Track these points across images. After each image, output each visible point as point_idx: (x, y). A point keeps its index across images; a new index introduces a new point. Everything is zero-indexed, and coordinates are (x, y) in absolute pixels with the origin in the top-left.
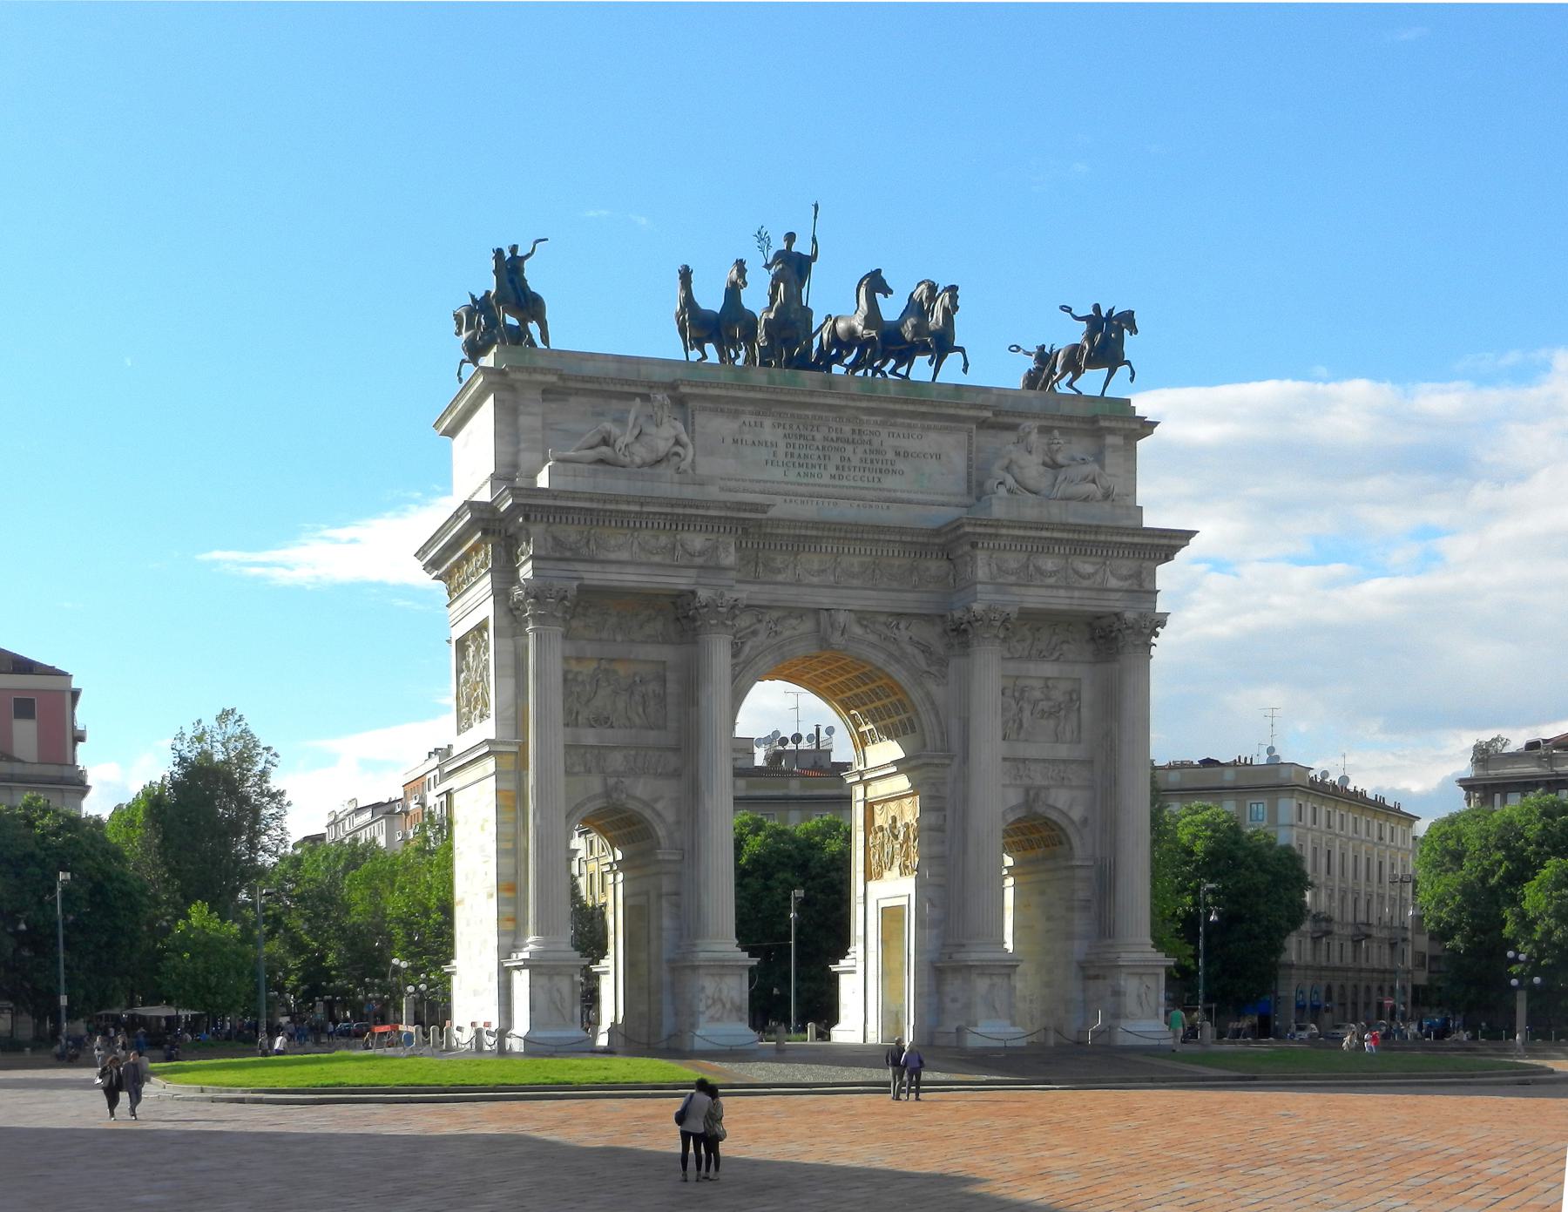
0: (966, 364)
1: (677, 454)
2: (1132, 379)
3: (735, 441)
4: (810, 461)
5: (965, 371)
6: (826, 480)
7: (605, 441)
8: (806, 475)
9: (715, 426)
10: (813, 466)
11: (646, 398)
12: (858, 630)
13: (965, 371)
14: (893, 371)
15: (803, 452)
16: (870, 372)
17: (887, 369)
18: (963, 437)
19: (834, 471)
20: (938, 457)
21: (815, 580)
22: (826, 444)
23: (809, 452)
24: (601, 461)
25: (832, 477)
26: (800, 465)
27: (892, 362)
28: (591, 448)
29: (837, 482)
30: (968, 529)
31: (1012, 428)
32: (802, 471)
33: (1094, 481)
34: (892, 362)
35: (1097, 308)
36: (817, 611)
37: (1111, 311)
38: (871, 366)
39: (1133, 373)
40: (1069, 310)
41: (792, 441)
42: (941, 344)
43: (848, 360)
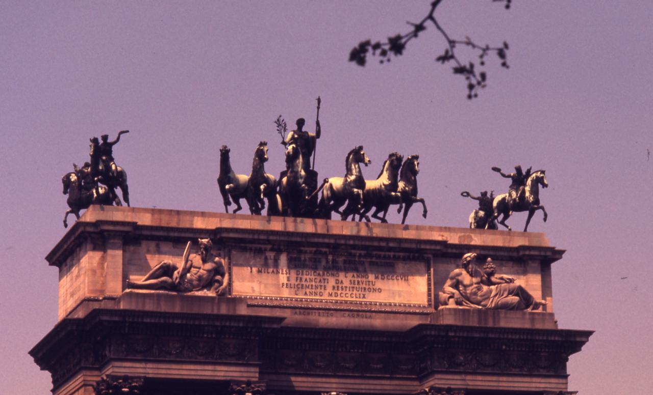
0: (425, 212)
2: (545, 220)
5: (425, 216)
6: (326, 297)
8: (311, 294)
10: (316, 287)
13: (425, 216)
14: (375, 216)
16: (357, 217)
17: (370, 214)
25: (331, 295)
26: (307, 287)
27: (374, 209)
32: (308, 291)
34: (374, 209)
35: (518, 170)
38: (359, 213)
39: (546, 215)
43: (342, 209)
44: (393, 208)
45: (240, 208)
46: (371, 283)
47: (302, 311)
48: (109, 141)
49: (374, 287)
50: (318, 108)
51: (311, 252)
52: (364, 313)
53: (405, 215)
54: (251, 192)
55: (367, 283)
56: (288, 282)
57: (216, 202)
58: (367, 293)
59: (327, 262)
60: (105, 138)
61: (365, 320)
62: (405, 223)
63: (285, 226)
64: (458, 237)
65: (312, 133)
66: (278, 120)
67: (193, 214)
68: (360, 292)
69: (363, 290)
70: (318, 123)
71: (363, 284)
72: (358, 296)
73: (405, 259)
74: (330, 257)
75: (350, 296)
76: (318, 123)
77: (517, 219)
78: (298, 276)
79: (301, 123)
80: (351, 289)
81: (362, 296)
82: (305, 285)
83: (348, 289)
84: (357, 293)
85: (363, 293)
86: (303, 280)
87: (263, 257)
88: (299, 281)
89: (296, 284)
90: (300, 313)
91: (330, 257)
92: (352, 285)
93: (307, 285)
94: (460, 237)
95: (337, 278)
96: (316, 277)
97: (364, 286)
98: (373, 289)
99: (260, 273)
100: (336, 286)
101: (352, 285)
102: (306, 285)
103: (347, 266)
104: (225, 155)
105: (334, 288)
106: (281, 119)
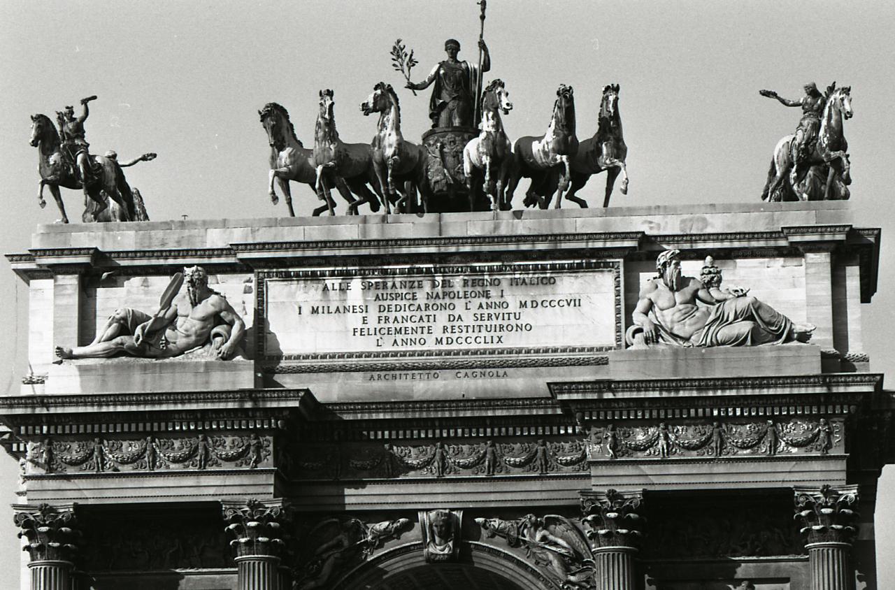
1: (218, 335)
3: (315, 311)
4: (409, 324)
6: (431, 346)
8: (404, 342)
10: (414, 331)
13: (625, 192)
15: (399, 315)
20: (576, 303)
22: (431, 302)
23: (408, 313)
25: (439, 341)
29: (444, 347)
32: (399, 337)
33: (750, 318)
37: (831, 89)
40: (774, 95)
41: (386, 303)
46: (512, 316)
47: (383, 373)
48: (78, 114)
49: (519, 322)
50: (483, 17)
51: (402, 272)
52: (494, 370)
54: (350, 174)
55: (506, 316)
56: (364, 326)
58: (504, 334)
59: (434, 286)
60: (71, 110)
61: (495, 381)
62: (610, 205)
63: (364, 232)
64: (679, 223)
65: (474, 64)
66: (395, 48)
67: (206, 225)
68: (492, 333)
69: (498, 329)
70: (482, 46)
71: (497, 318)
72: (489, 340)
73: (573, 269)
74: (439, 279)
75: (464, 342)
76: (482, 46)
78: (381, 314)
79: (453, 47)
80: (477, 329)
81: (496, 340)
82: (393, 329)
83: (470, 330)
84: (488, 335)
85: (500, 334)
86: (391, 320)
87: (321, 286)
88: (382, 322)
89: (378, 327)
90: (379, 377)
91: (439, 279)
92: (479, 323)
93: (398, 329)
94: (683, 221)
95: (451, 313)
96: (414, 313)
97: (500, 321)
98: (517, 326)
99: (315, 315)
100: (449, 325)
101: (479, 323)
102: (396, 329)
103: (470, 289)
105: (445, 329)
106: (401, 44)
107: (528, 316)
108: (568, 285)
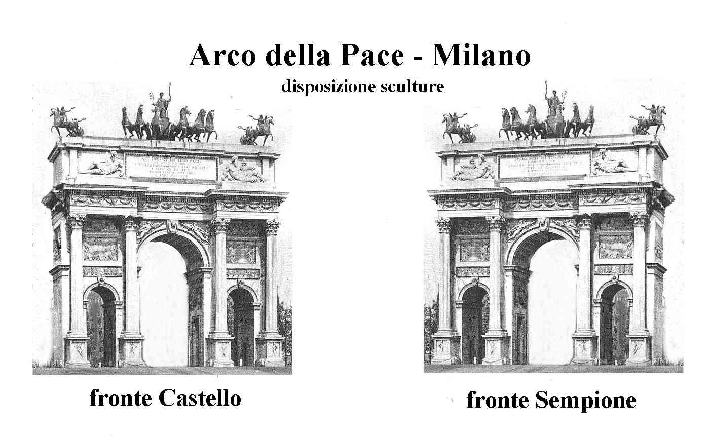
7: (96, 167)
9: (131, 160)
11: (109, 151)
12: (179, 227)
14: (195, 138)
17: (192, 138)
18: (214, 162)
19: (172, 174)
21: (165, 211)
24: (95, 174)
27: (194, 135)
28: (92, 169)
30: (213, 193)
31: (231, 157)
33: (256, 175)
34: (194, 135)
36: (166, 220)
42: (209, 131)
44: (202, 135)
45: (133, 135)
51: (163, 156)
53: (208, 137)
57: (119, 132)
70: (169, 95)
76: (169, 95)
77: (260, 140)
79: (161, 94)
104: (124, 110)
107: (194, 170)
108: (204, 163)
